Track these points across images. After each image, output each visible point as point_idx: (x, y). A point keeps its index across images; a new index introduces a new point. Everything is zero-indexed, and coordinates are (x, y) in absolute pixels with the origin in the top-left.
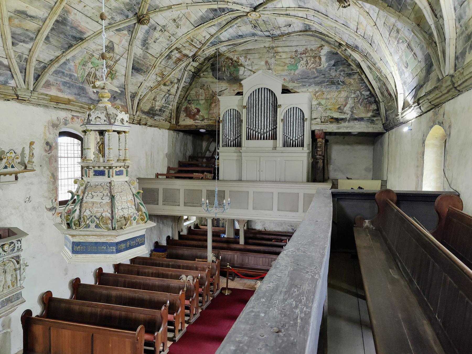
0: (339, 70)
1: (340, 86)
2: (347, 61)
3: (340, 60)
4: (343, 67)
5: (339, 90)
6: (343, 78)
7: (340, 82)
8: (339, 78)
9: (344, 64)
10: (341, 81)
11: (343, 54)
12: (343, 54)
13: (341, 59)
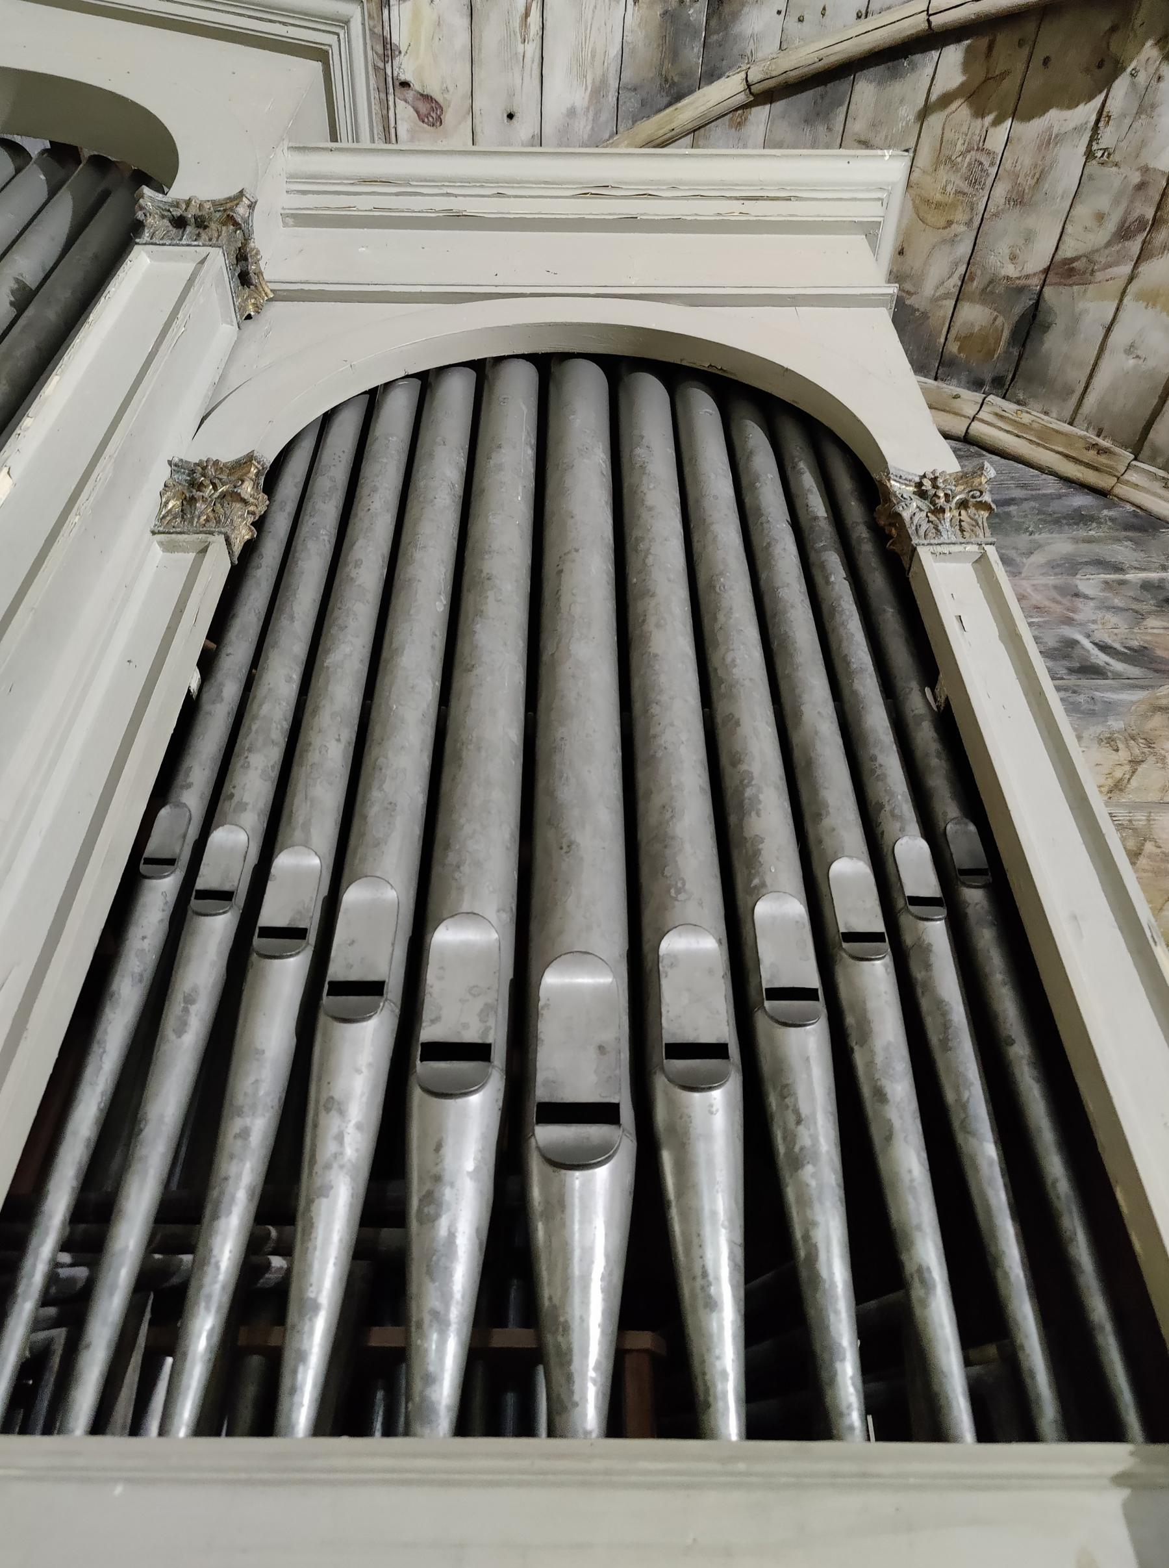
0: (1038, 558)
1: (1112, 689)
2: (1101, 493)
3: (1018, 493)
4: (1076, 540)
5: (1116, 724)
6: (1113, 619)
7: (1100, 658)
8: (1069, 621)
9: (1080, 518)
10: (1104, 648)
11: (1044, 437)
12: (1044, 437)
13: (1024, 486)
